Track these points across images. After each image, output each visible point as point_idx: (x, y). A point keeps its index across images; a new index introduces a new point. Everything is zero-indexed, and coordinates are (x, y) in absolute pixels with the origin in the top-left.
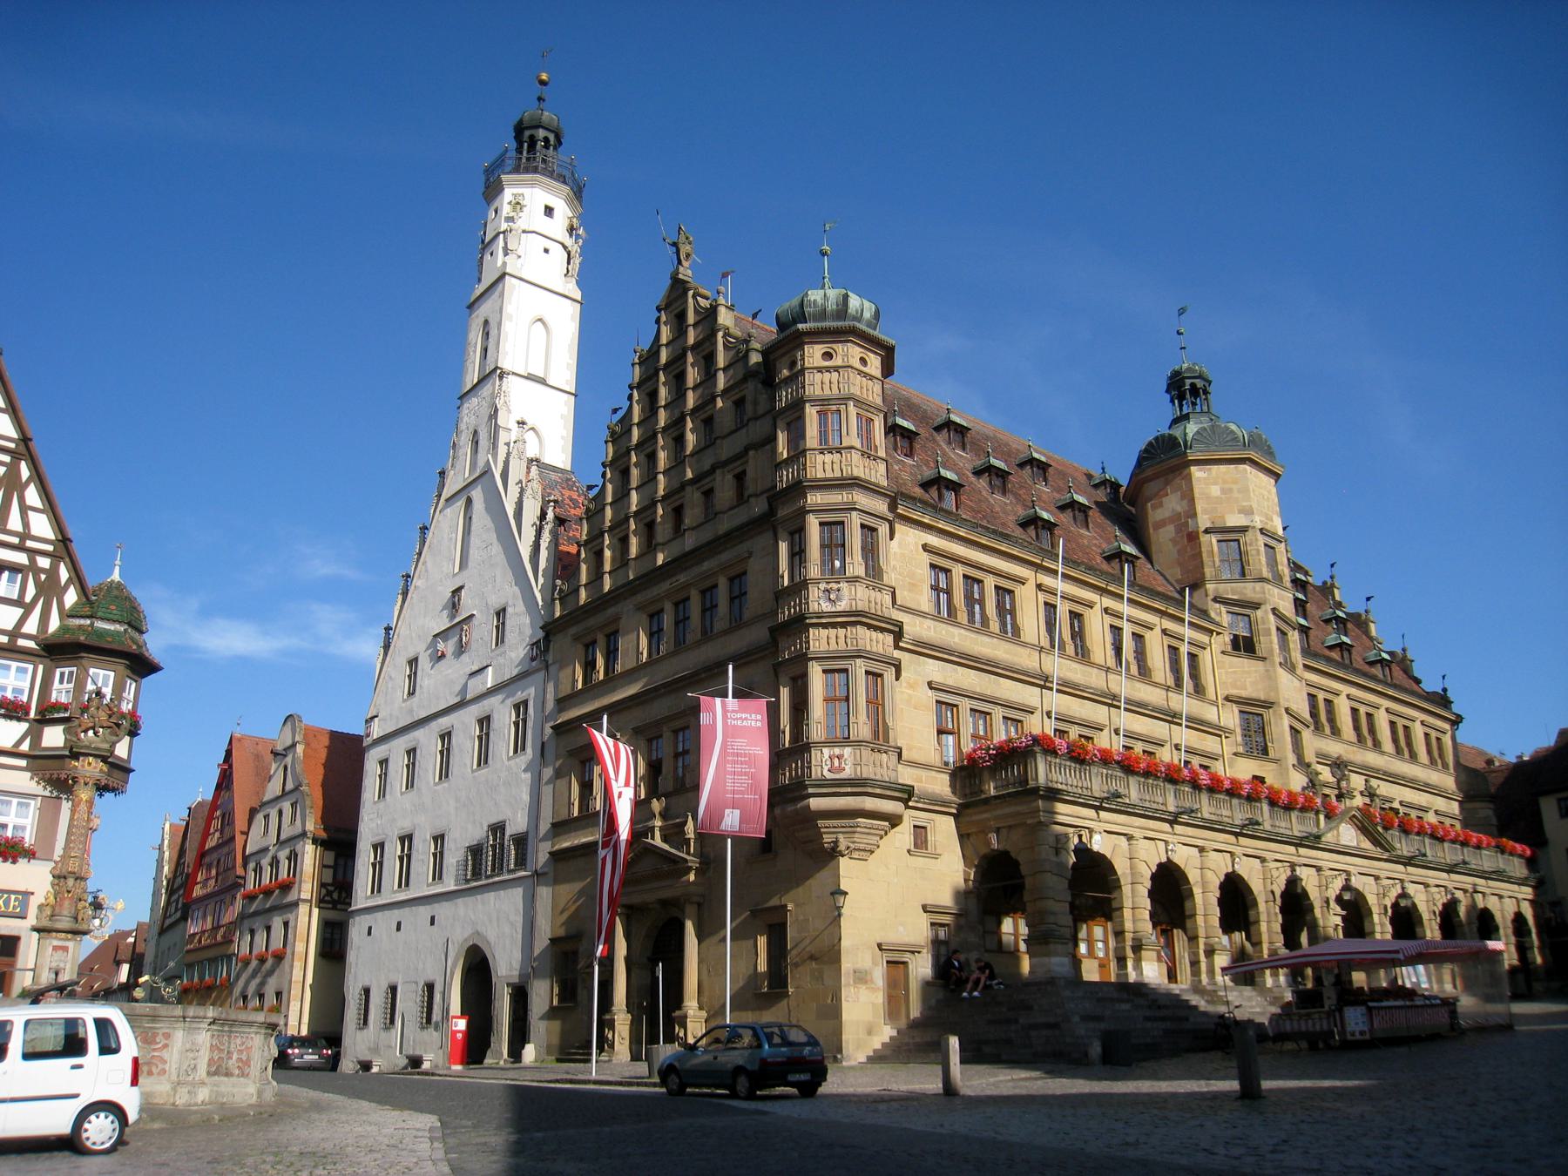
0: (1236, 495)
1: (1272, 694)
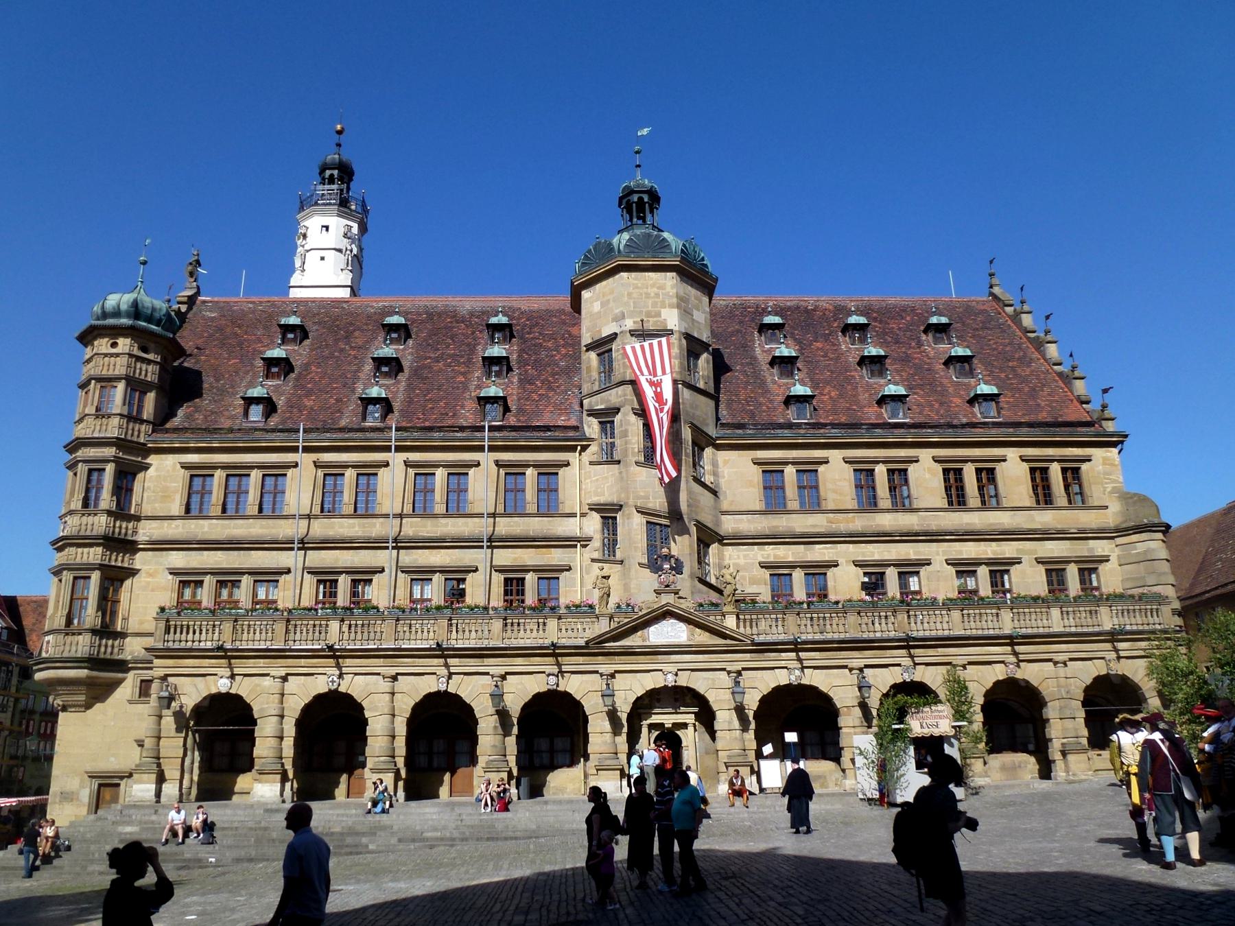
0: (612, 304)
1: (623, 495)
